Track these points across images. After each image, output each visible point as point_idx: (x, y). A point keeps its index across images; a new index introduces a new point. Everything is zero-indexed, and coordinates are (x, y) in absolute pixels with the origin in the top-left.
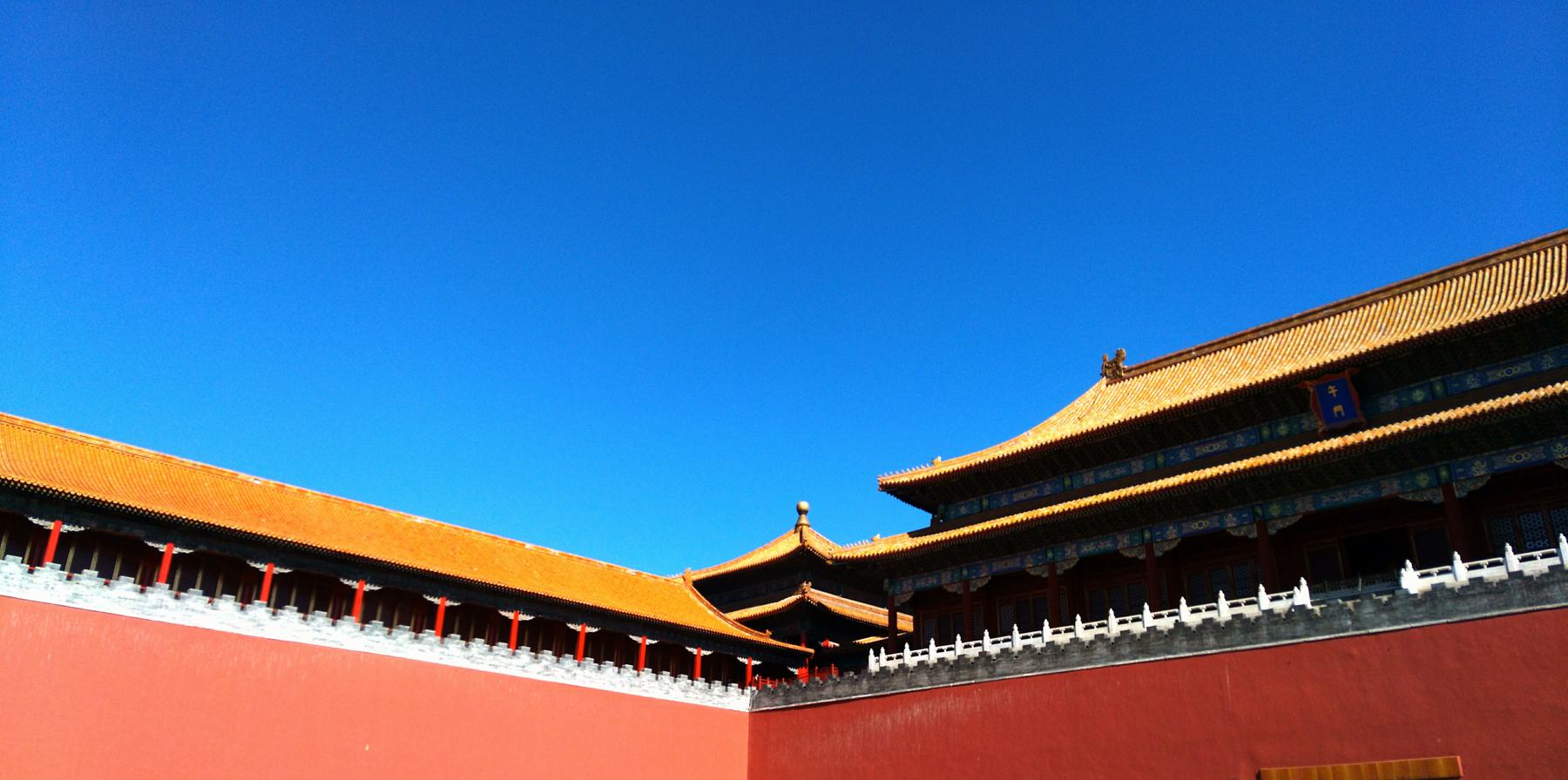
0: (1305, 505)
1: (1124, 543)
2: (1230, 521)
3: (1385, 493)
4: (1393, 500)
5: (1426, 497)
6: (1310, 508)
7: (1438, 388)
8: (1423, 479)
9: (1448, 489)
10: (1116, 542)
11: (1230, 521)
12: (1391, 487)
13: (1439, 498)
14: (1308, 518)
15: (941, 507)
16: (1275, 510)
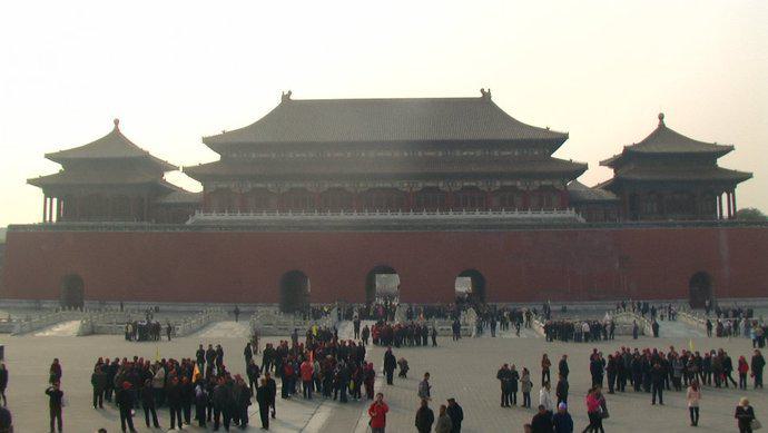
0: (370, 185)
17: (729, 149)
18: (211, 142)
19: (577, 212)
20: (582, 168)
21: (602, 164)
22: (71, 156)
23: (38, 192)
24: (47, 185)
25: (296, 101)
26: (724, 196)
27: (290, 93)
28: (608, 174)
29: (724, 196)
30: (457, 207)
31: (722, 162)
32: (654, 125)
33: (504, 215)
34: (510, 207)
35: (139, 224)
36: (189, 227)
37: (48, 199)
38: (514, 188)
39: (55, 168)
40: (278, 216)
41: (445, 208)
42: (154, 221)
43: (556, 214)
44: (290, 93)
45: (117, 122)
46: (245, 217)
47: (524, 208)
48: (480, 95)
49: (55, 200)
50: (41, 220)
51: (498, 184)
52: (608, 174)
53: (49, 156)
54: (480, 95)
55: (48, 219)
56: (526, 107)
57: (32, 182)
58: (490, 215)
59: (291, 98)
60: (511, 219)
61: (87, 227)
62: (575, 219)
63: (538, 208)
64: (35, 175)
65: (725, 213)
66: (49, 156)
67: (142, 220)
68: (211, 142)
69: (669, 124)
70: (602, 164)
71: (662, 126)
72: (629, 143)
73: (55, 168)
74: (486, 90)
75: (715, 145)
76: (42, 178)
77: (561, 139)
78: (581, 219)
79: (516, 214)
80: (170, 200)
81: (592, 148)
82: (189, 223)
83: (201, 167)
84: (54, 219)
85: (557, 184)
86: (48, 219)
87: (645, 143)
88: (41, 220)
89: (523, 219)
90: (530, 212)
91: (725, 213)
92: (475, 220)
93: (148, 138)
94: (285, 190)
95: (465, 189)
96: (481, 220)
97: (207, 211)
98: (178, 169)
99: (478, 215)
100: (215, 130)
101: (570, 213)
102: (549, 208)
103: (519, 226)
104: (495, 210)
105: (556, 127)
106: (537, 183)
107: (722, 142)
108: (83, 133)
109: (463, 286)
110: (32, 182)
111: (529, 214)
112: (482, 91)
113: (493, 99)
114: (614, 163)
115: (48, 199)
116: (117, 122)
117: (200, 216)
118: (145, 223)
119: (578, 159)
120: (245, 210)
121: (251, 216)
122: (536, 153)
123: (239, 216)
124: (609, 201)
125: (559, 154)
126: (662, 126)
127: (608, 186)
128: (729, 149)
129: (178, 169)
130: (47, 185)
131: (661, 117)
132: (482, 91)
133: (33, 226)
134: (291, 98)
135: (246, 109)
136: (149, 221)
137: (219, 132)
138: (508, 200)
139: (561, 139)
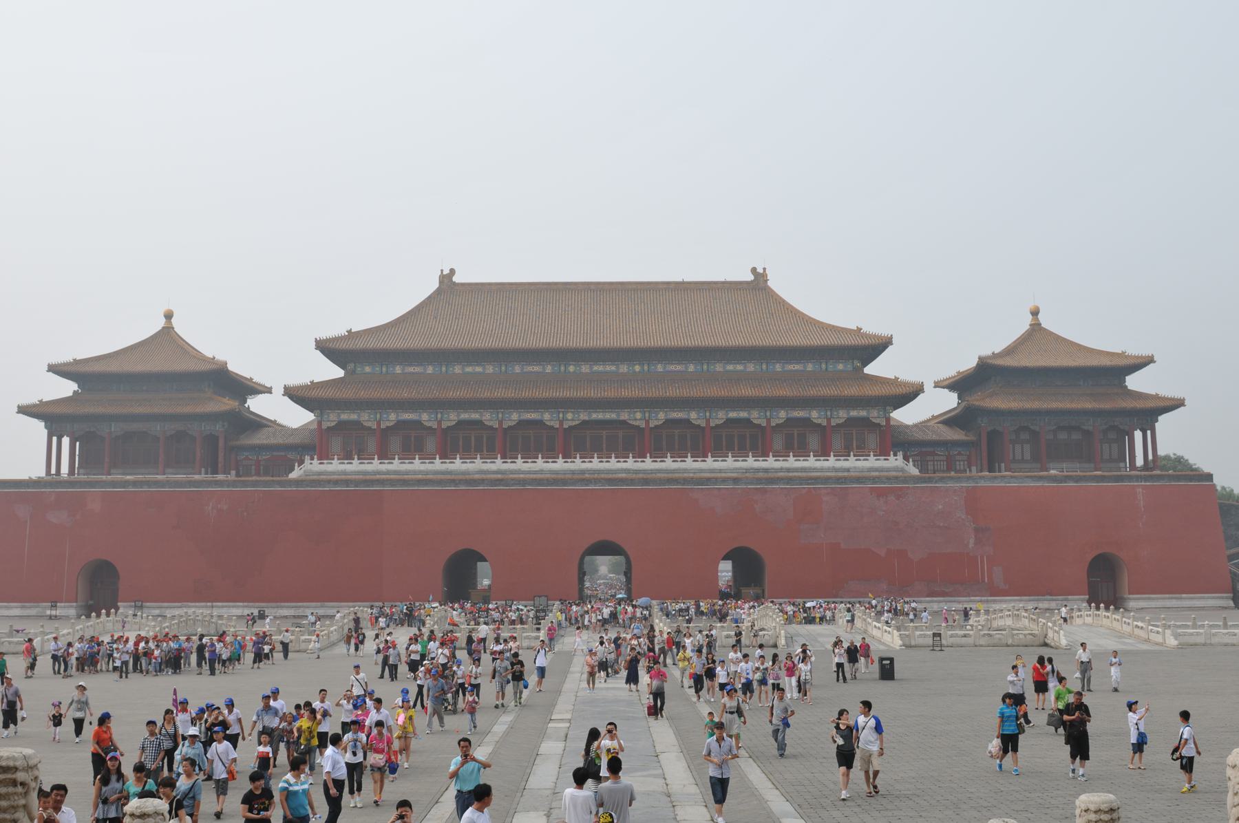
0: (584, 416)
1: (488, 417)
2: (547, 416)
3: (622, 418)
4: (624, 422)
5: (637, 423)
6: (586, 418)
7: (646, 368)
8: (638, 415)
9: (647, 422)
10: (481, 415)
11: (547, 416)
12: (624, 416)
13: (643, 426)
14: (584, 422)
15: (351, 366)
16: (570, 416)
17: (1148, 361)
18: (328, 349)
19: (906, 458)
20: (909, 394)
21: (937, 385)
22: (97, 368)
23: (38, 429)
24: (53, 417)
25: (463, 284)
26: (1138, 435)
28: (949, 401)
29: (1138, 435)
30: (719, 450)
31: (1134, 382)
32: (1024, 325)
33: (792, 462)
34: (802, 452)
35: (209, 477)
36: (297, 482)
37: (55, 439)
38: (807, 422)
39: (68, 388)
40: (438, 465)
41: (700, 452)
42: (233, 472)
43: (873, 462)
44: (452, 272)
45: (169, 316)
46: (385, 467)
47: (824, 452)
48: (750, 277)
49: (66, 441)
50: (42, 473)
51: (783, 414)
52: (949, 401)
53: (55, 369)
54: (750, 277)
55: (53, 471)
56: (825, 297)
57: (24, 410)
58: (771, 463)
59: (456, 279)
60: (803, 470)
61: (125, 484)
62: (902, 470)
63: (845, 453)
64: (32, 399)
65: (1140, 462)
66: (55, 369)
67: (215, 472)
68: (328, 349)
69: (1046, 322)
70: (937, 385)
71: (1036, 327)
72: (987, 351)
73: (68, 388)
75: (1122, 355)
76: (42, 403)
77: (877, 347)
78: (914, 471)
79: (812, 462)
80: (260, 439)
81: (926, 362)
82: (293, 475)
83: (314, 385)
84: (65, 469)
85: (874, 415)
86: (53, 471)
87: (1009, 351)
88: (42, 473)
89: (822, 470)
90: (832, 458)
91: (1140, 462)
92: (747, 470)
93: (211, 340)
94: (449, 424)
95: (729, 422)
96: (758, 470)
97: (324, 456)
98: (269, 391)
99: (751, 462)
100: (335, 329)
101: (895, 461)
102: (862, 452)
103: (816, 480)
104: (777, 455)
105: (874, 327)
106: (842, 415)
107: (1135, 349)
108: (110, 333)
109: (725, 571)
110: (24, 410)
111: (831, 462)
112: (754, 270)
113: (771, 284)
114: (960, 385)
115: (55, 439)
116: (169, 316)
117: (312, 466)
118: (220, 477)
119: (908, 374)
120: (384, 455)
121: (396, 465)
122: (841, 367)
123: (375, 465)
124: (955, 443)
125: (871, 369)
126: (1036, 327)
127: (951, 420)
128: (1148, 361)
129: (269, 391)
130: (53, 417)
131: (1035, 313)
132: (754, 270)
133: (37, 483)
134: (456, 279)
135: (381, 298)
136: (226, 472)
137: (341, 331)
138: (797, 438)
139: (877, 347)
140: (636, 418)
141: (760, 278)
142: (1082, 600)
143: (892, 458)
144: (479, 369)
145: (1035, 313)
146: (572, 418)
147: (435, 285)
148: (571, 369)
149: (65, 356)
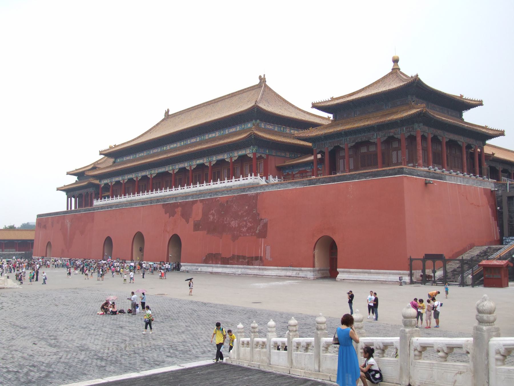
3: (167, 170)
23: (64, 195)
24: (70, 191)
27: (168, 110)
39: (75, 179)
44: (168, 110)
50: (65, 209)
53: (68, 173)
57: (58, 189)
59: (170, 113)
64: (61, 185)
66: (68, 173)
74: (263, 77)
84: (73, 208)
110: (58, 189)
112: (260, 77)
130: (70, 191)
134: (170, 113)
140: (169, 169)
141: (262, 80)
142: (310, 271)
143: (249, 177)
144: (142, 154)
145: (396, 61)
146: (155, 172)
147: (163, 117)
148: (165, 148)
149: (72, 169)
